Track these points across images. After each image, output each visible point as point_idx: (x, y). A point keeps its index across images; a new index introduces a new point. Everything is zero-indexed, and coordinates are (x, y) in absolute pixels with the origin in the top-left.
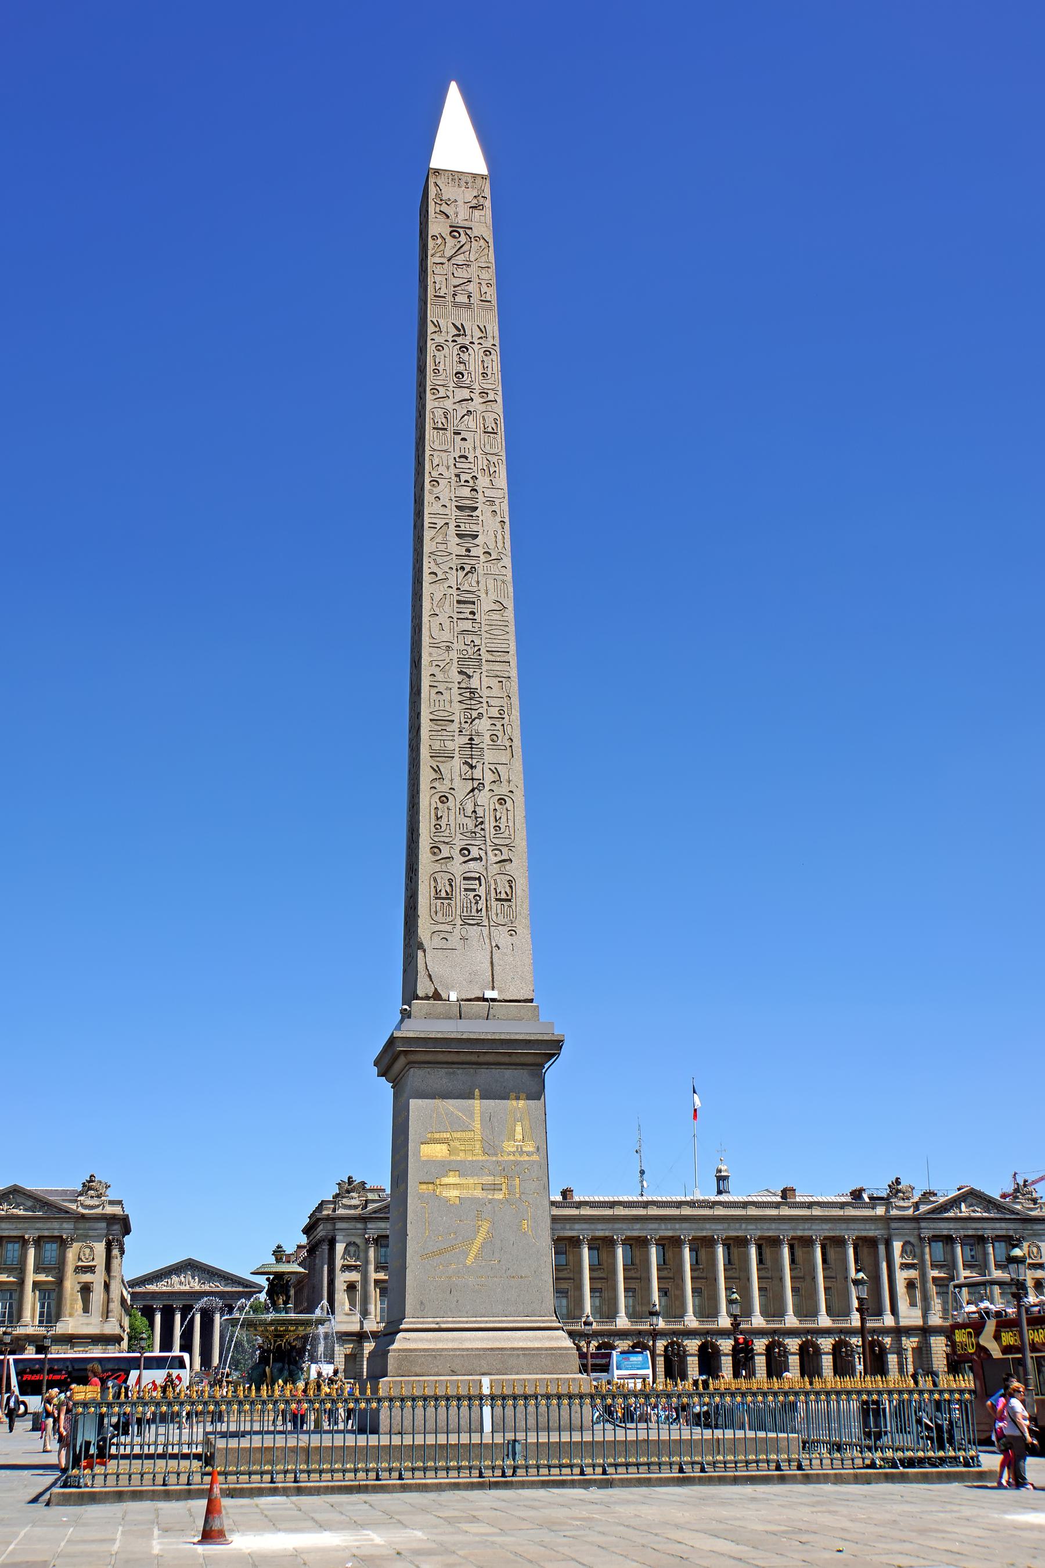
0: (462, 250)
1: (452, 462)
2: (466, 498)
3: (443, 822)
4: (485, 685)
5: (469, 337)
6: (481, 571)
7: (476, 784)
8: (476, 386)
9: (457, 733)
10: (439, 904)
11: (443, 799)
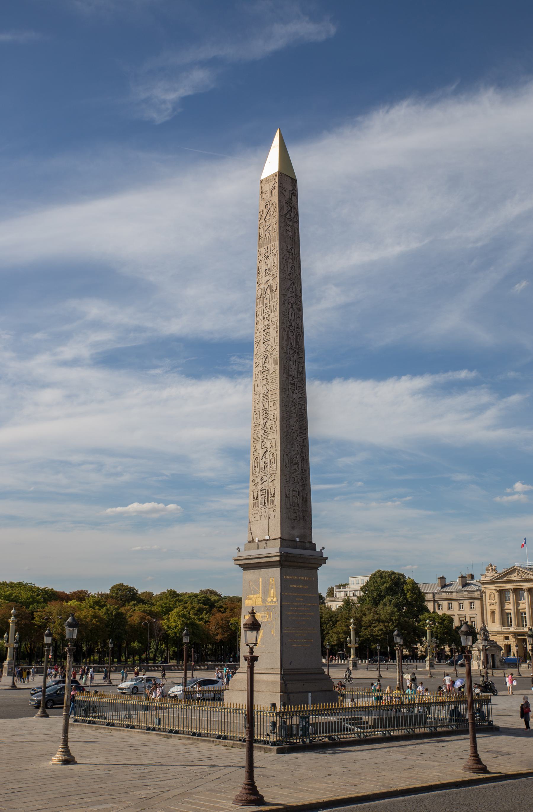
2: (266, 325)
4: (269, 406)
5: (269, 252)
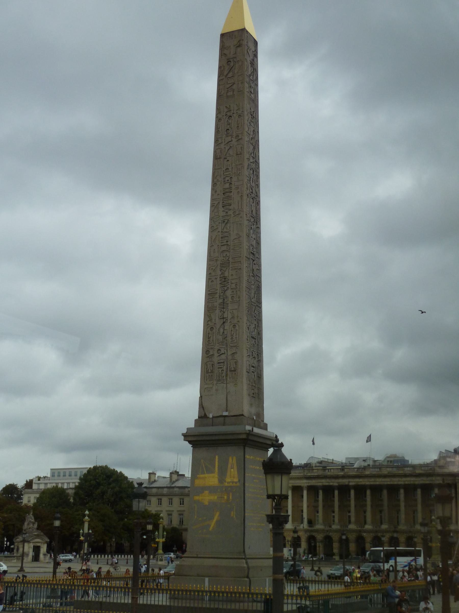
1: (222, 173)
2: (227, 188)
3: (211, 339)
4: (230, 274)
5: (232, 111)
7: (225, 320)
9: (218, 299)
11: (212, 328)
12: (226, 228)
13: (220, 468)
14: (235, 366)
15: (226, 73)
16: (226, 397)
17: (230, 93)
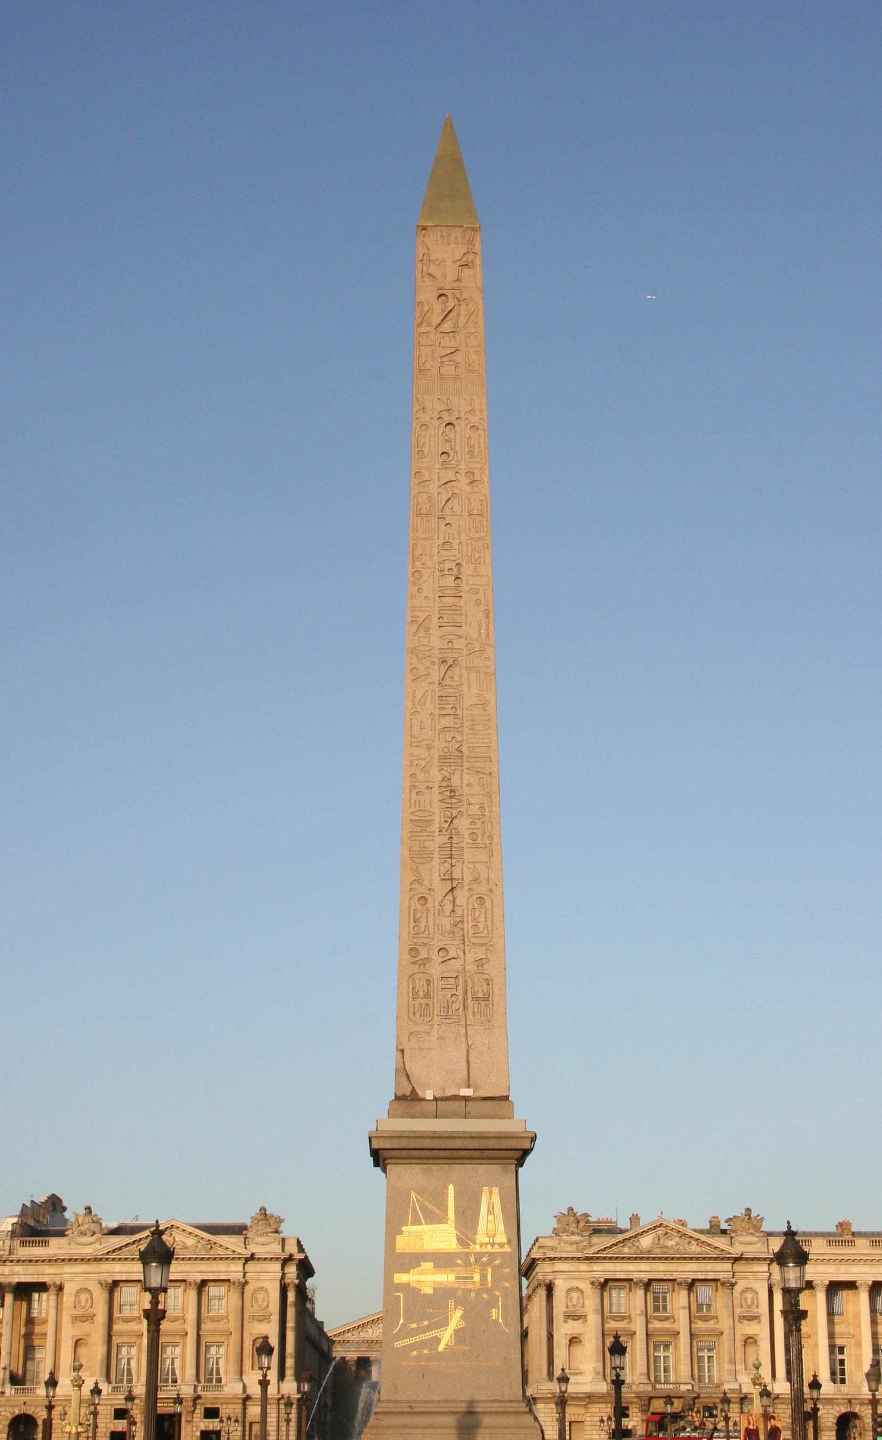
0: (450, 317)
1: (435, 550)
4: (465, 782)
5: (456, 414)
6: (463, 664)
8: (463, 466)
9: (437, 833)
10: (416, 1005)
12: (451, 677)
13: (461, 1214)
14: (485, 989)
15: (436, 320)
16: (465, 1056)
17: (448, 370)
